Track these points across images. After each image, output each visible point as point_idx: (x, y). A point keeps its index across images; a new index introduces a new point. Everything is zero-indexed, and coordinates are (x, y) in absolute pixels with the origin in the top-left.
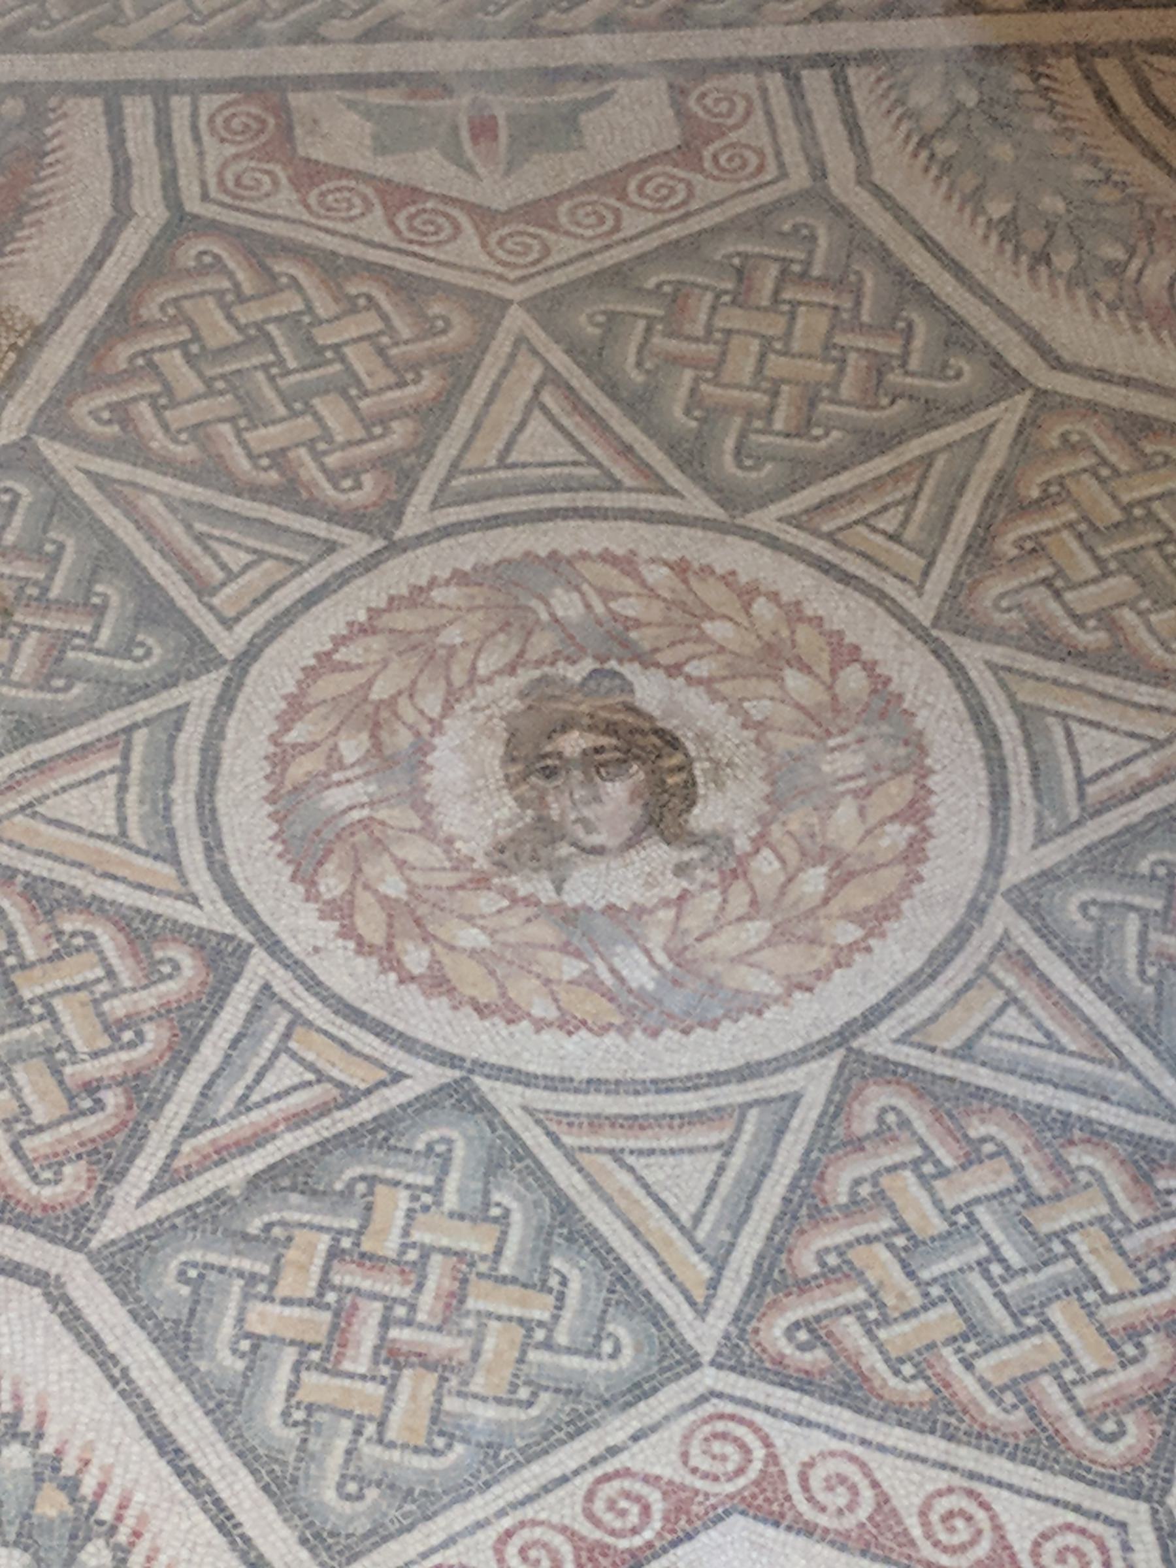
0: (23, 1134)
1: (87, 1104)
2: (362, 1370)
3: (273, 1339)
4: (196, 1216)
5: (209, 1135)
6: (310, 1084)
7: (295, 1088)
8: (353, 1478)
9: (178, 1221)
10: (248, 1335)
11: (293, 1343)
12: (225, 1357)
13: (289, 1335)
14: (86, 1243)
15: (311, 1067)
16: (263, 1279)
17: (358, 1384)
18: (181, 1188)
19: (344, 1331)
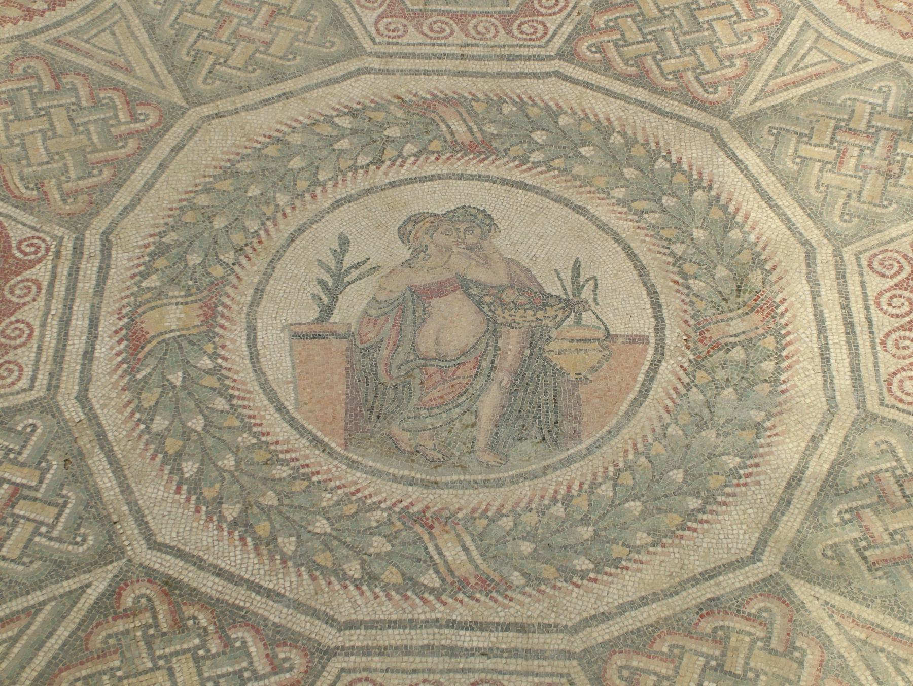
0: (700, 74)
1: (728, 64)
2: (850, 173)
3: (811, 159)
4: (776, 110)
5: (782, 79)
6: (826, 61)
7: (819, 63)
8: (847, 214)
9: (769, 112)
10: (799, 157)
11: (819, 161)
12: (790, 164)
13: (818, 158)
14: (728, 117)
15: (826, 55)
16: (806, 136)
17: (849, 178)
18: (769, 99)
19: (842, 158)
